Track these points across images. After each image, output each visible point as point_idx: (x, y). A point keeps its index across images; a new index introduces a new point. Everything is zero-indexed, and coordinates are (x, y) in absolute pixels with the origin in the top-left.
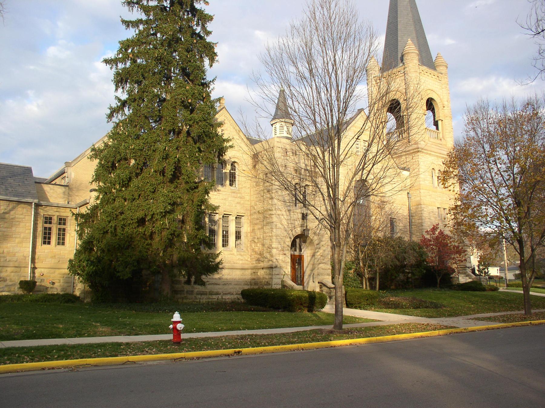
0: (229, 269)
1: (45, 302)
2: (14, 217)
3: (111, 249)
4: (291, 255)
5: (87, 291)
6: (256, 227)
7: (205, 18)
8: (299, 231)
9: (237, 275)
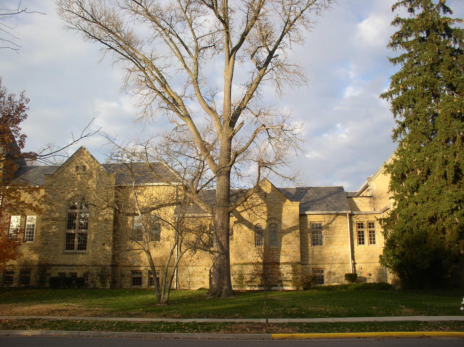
1: (365, 289)
2: (335, 226)
3: (409, 245)
5: (397, 280)
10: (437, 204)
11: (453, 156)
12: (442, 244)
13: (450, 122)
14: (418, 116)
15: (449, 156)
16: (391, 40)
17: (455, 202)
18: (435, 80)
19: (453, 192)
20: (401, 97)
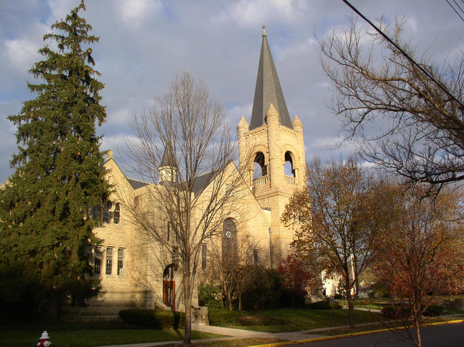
0: (111, 292)
4: (164, 282)
6: (135, 258)
7: (97, 86)
8: (170, 261)
9: (117, 298)
10: (40, 237)
11: (65, 194)
12: (37, 278)
13: (69, 162)
14: (41, 148)
15: (61, 193)
16: (35, 67)
17: (58, 239)
18: (66, 118)
19: (57, 228)
20: (29, 125)
